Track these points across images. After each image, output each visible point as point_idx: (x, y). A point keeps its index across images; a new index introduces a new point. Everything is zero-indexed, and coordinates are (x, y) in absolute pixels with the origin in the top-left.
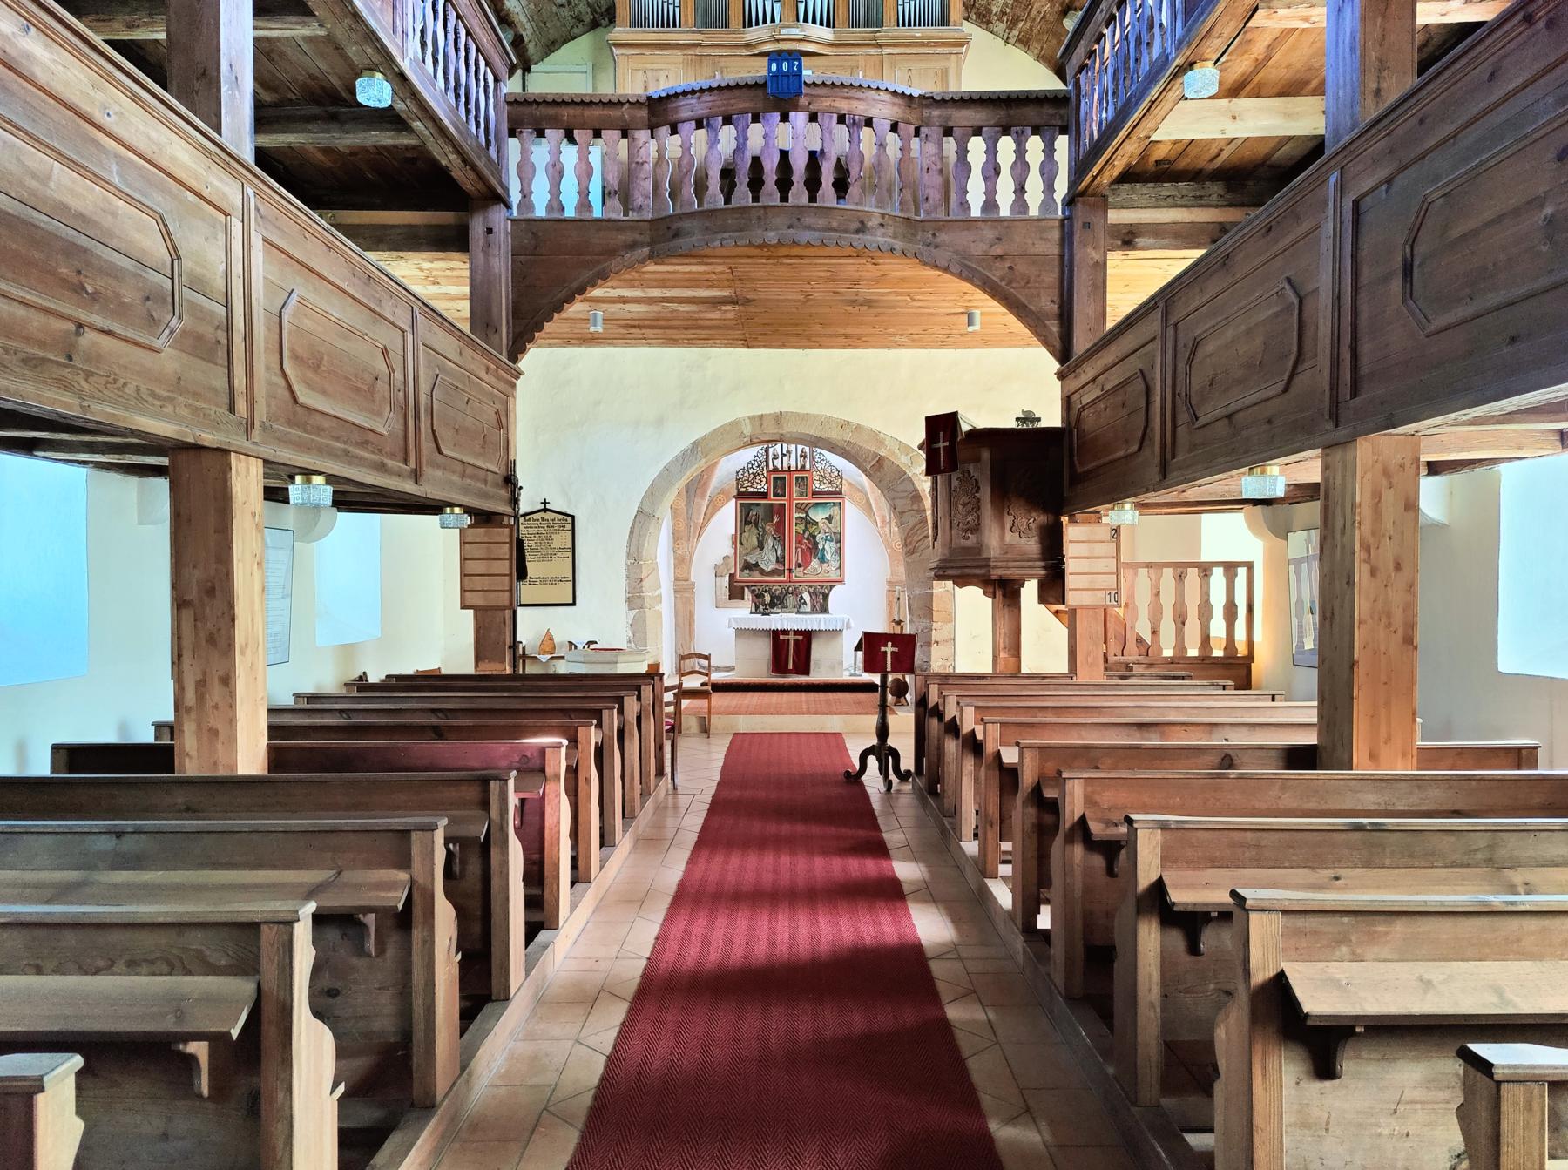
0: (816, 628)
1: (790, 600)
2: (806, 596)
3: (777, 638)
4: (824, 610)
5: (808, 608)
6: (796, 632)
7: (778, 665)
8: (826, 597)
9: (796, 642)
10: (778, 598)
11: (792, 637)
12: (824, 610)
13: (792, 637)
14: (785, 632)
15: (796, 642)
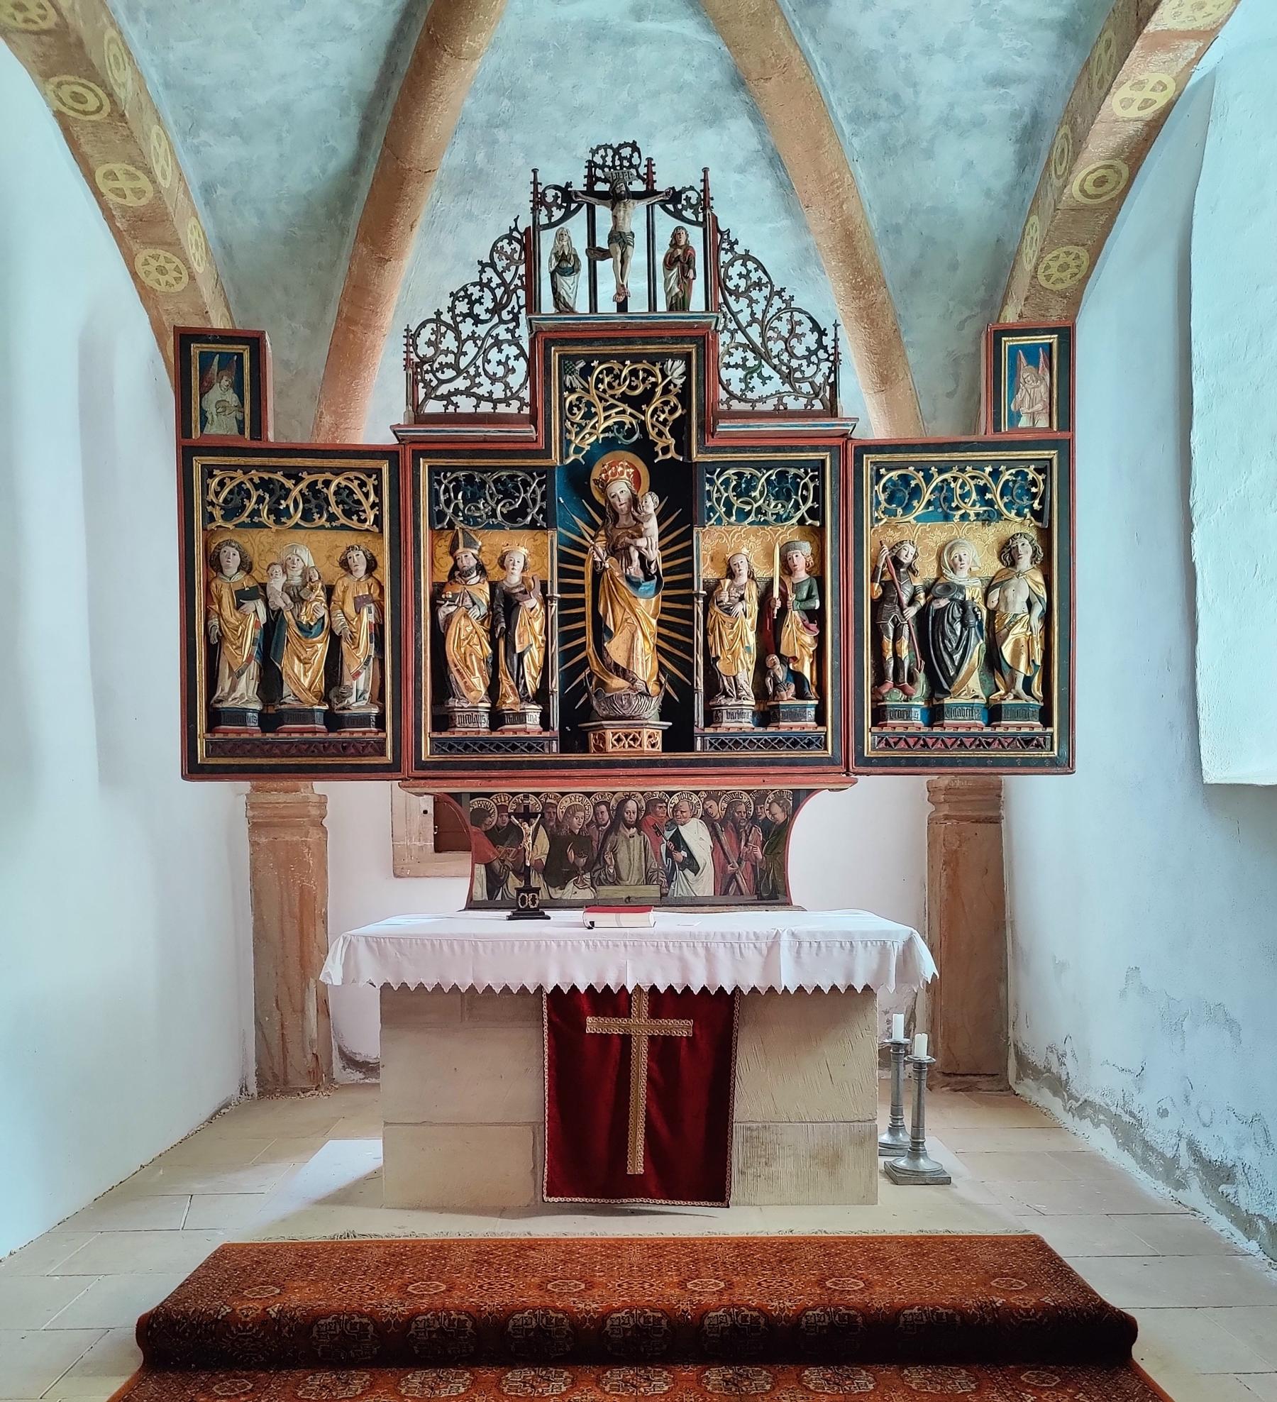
0: (751, 979)
1: (630, 851)
2: (696, 836)
3: (571, 1022)
4: (770, 890)
5: (704, 884)
6: (665, 1002)
7: (582, 1161)
8: (777, 837)
9: (662, 1047)
10: (581, 841)
11: (641, 1027)
12: (770, 890)
13: (641, 1027)
14: (610, 1001)
15: (662, 1047)
